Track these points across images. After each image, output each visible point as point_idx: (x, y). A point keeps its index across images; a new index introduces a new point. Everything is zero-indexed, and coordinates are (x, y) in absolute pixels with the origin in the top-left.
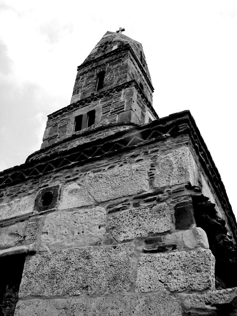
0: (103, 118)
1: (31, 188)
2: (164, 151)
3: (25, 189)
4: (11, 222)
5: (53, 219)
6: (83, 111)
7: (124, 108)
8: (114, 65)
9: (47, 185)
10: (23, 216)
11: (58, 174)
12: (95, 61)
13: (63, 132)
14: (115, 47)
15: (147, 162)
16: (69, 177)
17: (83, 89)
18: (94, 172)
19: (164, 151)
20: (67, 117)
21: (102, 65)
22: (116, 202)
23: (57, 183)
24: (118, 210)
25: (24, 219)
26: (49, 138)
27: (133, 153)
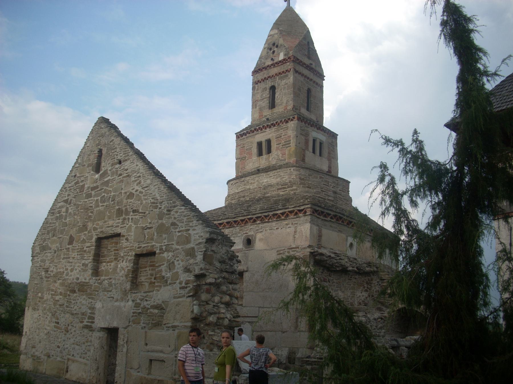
0: (277, 149)
1: (239, 233)
2: (300, 224)
6: (261, 137)
7: (290, 143)
11: (251, 227)
12: (265, 68)
14: (281, 57)
15: (292, 229)
18: (270, 230)
19: (300, 224)
20: (250, 140)
22: (280, 249)
24: (281, 254)
27: (286, 222)
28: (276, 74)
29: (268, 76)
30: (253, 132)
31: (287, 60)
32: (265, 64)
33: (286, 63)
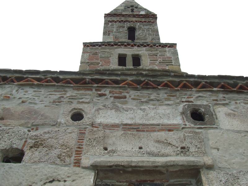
3: (158, 98)
4: (152, 128)
5: (218, 136)
8: (131, 25)
9: (192, 102)
10: (170, 125)
12: (123, 16)
13: (106, 62)
16: (217, 100)
17: (114, 33)
21: (132, 21)
23: (205, 103)
25: (173, 129)
26: (89, 63)
28: (136, 21)
29: (126, 20)
30: (112, 45)
31: (150, 16)
32: (122, 13)
33: (148, 17)
